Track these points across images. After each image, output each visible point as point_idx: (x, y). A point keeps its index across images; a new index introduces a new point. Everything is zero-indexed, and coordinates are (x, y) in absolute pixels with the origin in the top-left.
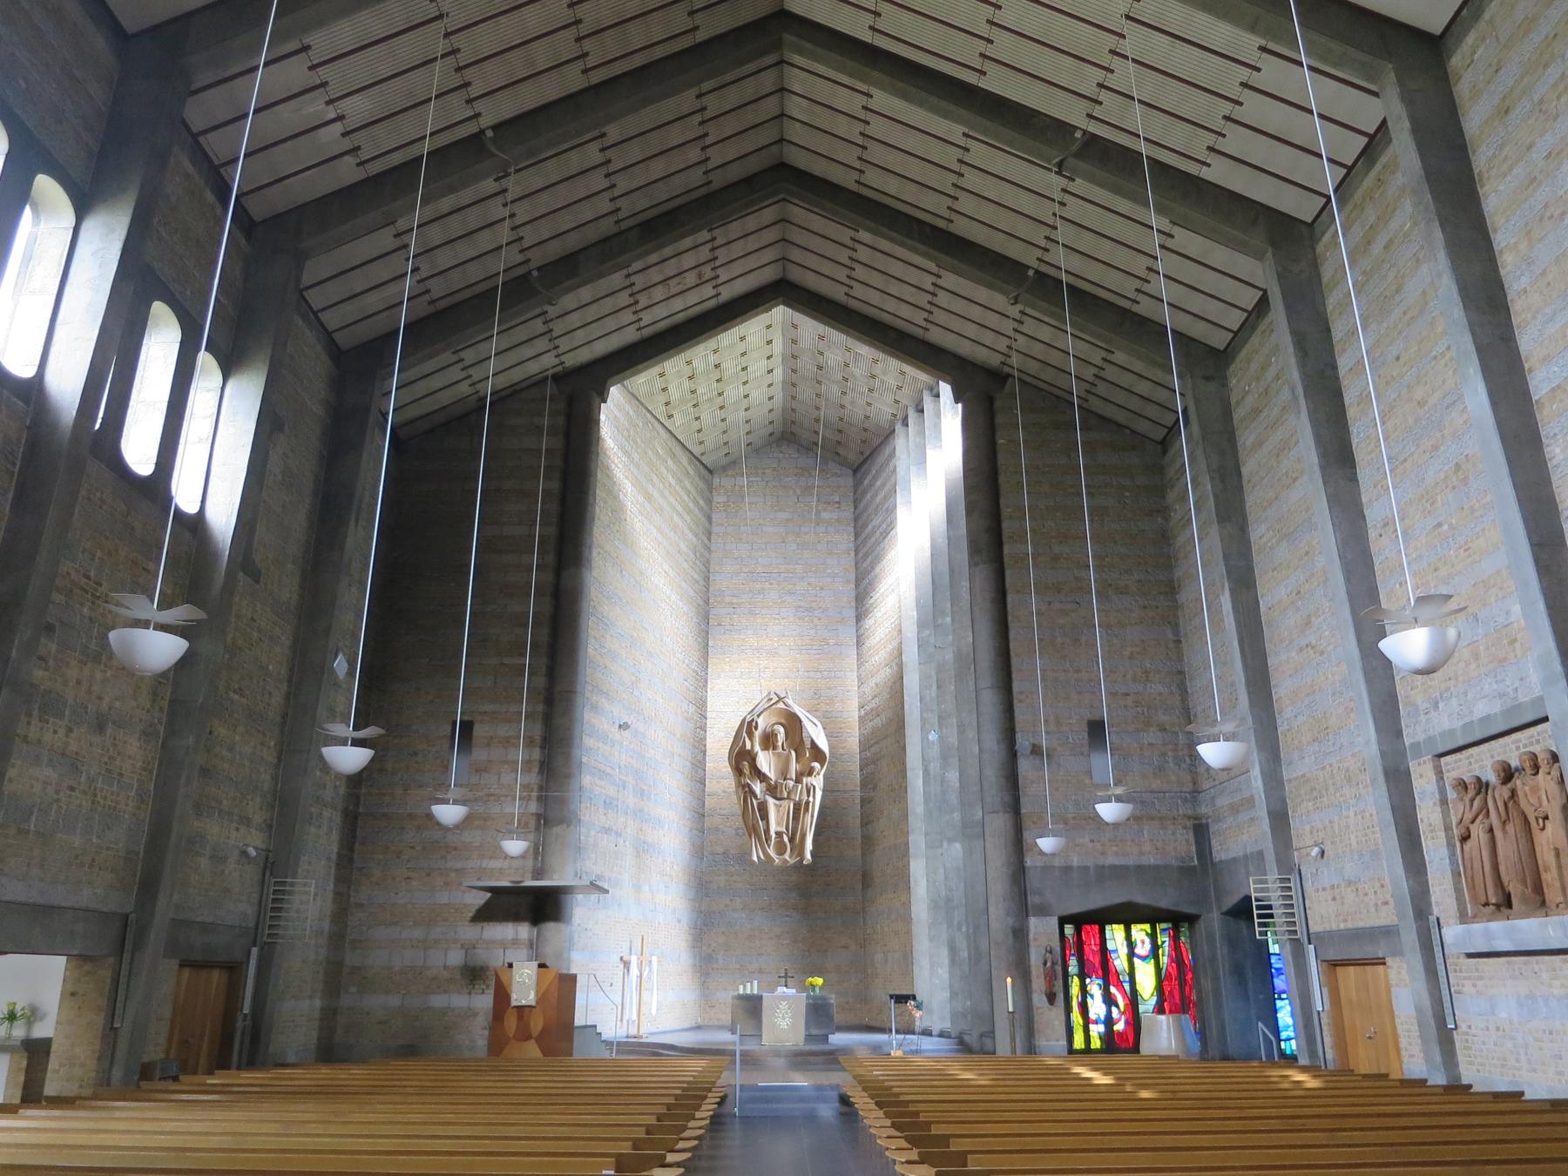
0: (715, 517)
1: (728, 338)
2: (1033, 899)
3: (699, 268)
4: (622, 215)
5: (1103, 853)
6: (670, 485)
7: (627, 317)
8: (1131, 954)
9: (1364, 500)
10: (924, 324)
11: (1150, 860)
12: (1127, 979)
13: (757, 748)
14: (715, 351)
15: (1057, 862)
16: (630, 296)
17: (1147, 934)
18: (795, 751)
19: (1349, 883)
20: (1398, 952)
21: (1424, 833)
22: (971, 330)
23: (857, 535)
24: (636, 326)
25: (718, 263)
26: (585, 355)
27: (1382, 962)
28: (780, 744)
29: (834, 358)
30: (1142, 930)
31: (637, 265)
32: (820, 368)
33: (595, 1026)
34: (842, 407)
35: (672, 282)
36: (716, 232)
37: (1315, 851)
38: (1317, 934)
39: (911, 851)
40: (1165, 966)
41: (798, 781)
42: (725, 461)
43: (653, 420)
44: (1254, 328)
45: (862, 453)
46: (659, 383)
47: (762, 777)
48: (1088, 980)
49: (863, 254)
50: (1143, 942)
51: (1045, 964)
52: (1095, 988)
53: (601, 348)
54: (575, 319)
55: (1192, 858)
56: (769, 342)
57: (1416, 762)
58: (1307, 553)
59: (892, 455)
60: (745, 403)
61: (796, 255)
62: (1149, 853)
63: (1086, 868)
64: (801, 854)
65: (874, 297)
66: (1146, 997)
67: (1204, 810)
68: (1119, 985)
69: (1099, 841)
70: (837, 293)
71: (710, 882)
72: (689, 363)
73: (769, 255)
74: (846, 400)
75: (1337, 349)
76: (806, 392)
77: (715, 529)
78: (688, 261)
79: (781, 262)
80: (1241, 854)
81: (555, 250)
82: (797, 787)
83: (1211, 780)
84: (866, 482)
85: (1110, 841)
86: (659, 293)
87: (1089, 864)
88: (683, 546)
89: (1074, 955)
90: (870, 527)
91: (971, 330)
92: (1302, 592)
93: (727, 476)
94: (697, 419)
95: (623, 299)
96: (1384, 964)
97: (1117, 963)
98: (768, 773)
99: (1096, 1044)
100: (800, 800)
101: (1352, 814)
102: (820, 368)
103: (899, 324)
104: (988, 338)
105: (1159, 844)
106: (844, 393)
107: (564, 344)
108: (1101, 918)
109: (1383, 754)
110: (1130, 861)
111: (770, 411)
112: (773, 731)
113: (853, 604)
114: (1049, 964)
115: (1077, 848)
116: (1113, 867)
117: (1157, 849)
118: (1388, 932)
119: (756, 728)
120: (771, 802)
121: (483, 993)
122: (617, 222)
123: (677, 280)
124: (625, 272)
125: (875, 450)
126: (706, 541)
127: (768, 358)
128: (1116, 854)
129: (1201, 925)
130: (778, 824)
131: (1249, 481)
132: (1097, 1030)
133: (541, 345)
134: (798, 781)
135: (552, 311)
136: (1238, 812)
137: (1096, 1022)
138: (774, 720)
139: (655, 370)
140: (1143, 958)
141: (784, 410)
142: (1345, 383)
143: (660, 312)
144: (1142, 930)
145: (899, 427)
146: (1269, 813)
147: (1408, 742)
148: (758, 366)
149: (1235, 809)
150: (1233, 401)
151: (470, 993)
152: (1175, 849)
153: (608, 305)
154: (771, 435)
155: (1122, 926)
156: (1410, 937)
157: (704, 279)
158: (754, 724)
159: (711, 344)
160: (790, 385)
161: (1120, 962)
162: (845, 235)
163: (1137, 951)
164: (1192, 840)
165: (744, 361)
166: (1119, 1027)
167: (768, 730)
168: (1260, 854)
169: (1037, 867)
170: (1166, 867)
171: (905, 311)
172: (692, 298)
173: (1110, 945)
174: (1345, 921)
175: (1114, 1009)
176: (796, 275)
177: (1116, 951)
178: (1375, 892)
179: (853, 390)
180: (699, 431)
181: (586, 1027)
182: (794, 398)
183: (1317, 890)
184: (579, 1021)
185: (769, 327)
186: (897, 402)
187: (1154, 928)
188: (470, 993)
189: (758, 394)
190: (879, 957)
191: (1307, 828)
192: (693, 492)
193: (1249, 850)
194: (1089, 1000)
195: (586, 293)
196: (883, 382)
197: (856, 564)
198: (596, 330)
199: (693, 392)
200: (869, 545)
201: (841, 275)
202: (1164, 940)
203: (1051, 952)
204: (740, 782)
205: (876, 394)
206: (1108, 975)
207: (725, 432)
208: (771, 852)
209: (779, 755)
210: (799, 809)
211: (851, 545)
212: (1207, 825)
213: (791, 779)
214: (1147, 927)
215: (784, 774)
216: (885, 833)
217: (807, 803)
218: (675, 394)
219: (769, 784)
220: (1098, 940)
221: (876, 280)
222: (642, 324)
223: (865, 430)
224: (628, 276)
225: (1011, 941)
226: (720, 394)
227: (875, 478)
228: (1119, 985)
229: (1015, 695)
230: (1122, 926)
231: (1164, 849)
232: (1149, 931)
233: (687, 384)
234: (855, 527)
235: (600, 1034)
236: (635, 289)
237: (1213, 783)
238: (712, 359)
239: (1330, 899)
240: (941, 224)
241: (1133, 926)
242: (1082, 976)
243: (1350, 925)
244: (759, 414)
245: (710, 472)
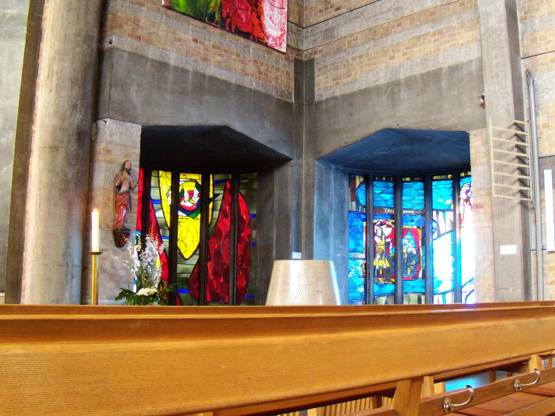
5: (205, 60)
8: (176, 207)
11: (251, 83)
12: (168, 234)
17: (197, 185)
30: (192, 180)
40: (215, 221)
50: (191, 193)
51: (119, 187)
63: (184, 71)
66: (187, 256)
69: (203, 44)
85: (214, 47)
97: (159, 214)
105: (263, 68)
110: (233, 78)
114: (124, 188)
115: (177, 44)
116: (212, 79)
117: (260, 73)
140: (189, 212)
144: (192, 180)
152: (277, 78)
155: (169, 175)
163: (182, 203)
169: (125, 51)
170: (267, 96)
173: (154, 194)
177: (160, 201)
187: (205, 180)
203: (129, 172)
214: (197, 177)
225: (73, 147)
230: (169, 175)
231: (267, 75)
241: (182, 176)
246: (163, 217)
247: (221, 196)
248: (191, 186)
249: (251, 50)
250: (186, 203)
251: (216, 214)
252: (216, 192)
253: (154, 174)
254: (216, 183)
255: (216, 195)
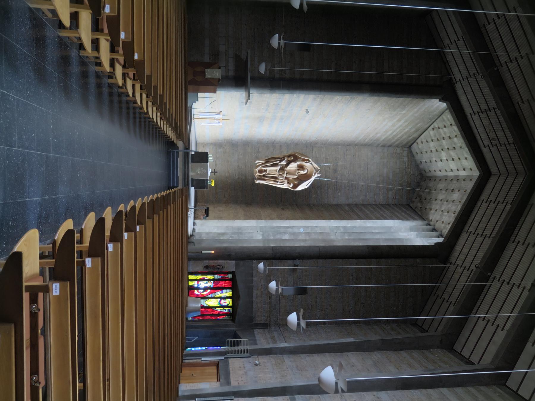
0: (391, 148)
1: (466, 152)
2: (241, 262)
3: (497, 138)
4: (521, 105)
6: (404, 129)
7: (476, 109)
8: (221, 298)
9: (389, 392)
10: (469, 231)
11: (255, 305)
12: (213, 296)
13: (298, 163)
14: (461, 147)
15: (254, 272)
16: (485, 110)
17: (228, 304)
18: (297, 178)
19: (246, 373)
20: (221, 385)
21: (263, 398)
22: (466, 250)
23: (382, 205)
24: (472, 113)
25: (499, 147)
26: (460, 92)
27: (218, 380)
28: (300, 172)
29: (456, 196)
30: (230, 302)
31: (498, 112)
32: (453, 190)
33: (198, 101)
34: (436, 200)
35: (491, 127)
36: (512, 145)
37: (257, 362)
38: (228, 361)
39: (259, 221)
40: (217, 310)
41: (286, 178)
42: (414, 152)
43: (432, 122)
44: (462, 360)
45: (416, 208)
46: (447, 124)
47: (287, 165)
48: (212, 282)
49: (501, 207)
50: (225, 303)
51: (218, 266)
52: (210, 284)
53: (463, 99)
54: (475, 87)
55: (255, 322)
56: (464, 170)
57: (288, 398)
58: (368, 370)
59: (414, 219)
60: (438, 160)
61: (502, 179)
62: (257, 306)
63: (252, 283)
64: (259, 179)
65: (481, 211)
66: (206, 302)
67: (273, 327)
68: (210, 293)
69: (262, 288)
70: (484, 196)
71: (248, 146)
72: (456, 136)
73: (502, 168)
74: (438, 201)
75: (451, 389)
76: (442, 185)
77: (386, 149)
78: (500, 134)
79: (498, 173)
80: (256, 338)
81: (507, 76)
82: (284, 178)
83: (284, 331)
84: (404, 209)
85: (262, 292)
86: (486, 122)
87: (254, 283)
88: (379, 135)
89: (221, 277)
90: (385, 210)
91: (466, 250)
92: (353, 367)
93: (408, 153)
94: (432, 141)
95: (484, 107)
96: (218, 381)
97: (218, 293)
98: (289, 167)
99: (190, 283)
100: (278, 179)
101: (270, 376)
102: (453, 190)
103: (469, 222)
104: (462, 257)
106: (441, 200)
107: (465, 83)
108: (234, 288)
109: (292, 387)
110: (254, 299)
111: (435, 171)
112: (305, 169)
113: (354, 203)
114: (218, 267)
115: (259, 280)
118: (228, 383)
119: (306, 163)
120: (278, 168)
121: (209, 59)
122: (518, 103)
123: (492, 129)
124: (496, 107)
125: (417, 212)
126: (381, 145)
127: (458, 170)
128: (257, 294)
129: (231, 323)
130: (270, 171)
131: (398, 353)
132: (195, 284)
133: (465, 73)
134: (286, 178)
135: (479, 77)
136: (272, 339)
137: (198, 284)
138: (309, 169)
139: (453, 122)
140: (220, 302)
141: (435, 176)
142: (437, 390)
143: (478, 123)
144: (230, 302)
145: (426, 222)
146: (271, 348)
147: (296, 396)
148: (454, 165)
149: (273, 338)
150: (432, 350)
151: (209, 54)
153: (481, 100)
154: (425, 171)
155: (231, 295)
156: (226, 389)
157: (492, 141)
158: (308, 162)
159: (464, 145)
160: (446, 178)
161: (219, 294)
162: (510, 199)
163: (222, 300)
164: (262, 322)
165: (456, 159)
166: (196, 292)
167: (305, 167)
168: (257, 344)
169: (253, 265)
171: (475, 224)
172: (484, 136)
173: (224, 291)
174: (233, 370)
175: (202, 291)
176: (493, 180)
178: (242, 381)
179: (443, 204)
180: (427, 141)
181: (198, 97)
182: (440, 180)
183: (243, 362)
184: (200, 94)
185: (471, 169)
186: (437, 221)
187: (230, 307)
188: (209, 54)
189: (442, 166)
190: (221, 208)
191: (265, 361)
192: (402, 139)
193: (257, 341)
194: (206, 282)
195: (487, 91)
196: (446, 216)
197: (370, 205)
198: (471, 96)
199: (444, 138)
200: (377, 209)
201: (492, 198)
202: (226, 310)
204: (286, 156)
205: (440, 213)
206: (215, 289)
207: (426, 152)
208: (259, 168)
209: (295, 171)
210: (275, 179)
211: (378, 203)
212: (268, 328)
213: (286, 176)
214: (231, 305)
215: (289, 173)
216: (266, 212)
217: (277, 182)
218: (443, 130)
219: (284, 168)
220: (226, 286)
221: (489, 212)
222: (473, 116)
223: (426, 209)
224: (494, 108)
226: (442, 150)
227: (405, 212)
228: (210, 293)
229: (317, 260)
230: (231, 295)
232: (229, 305)
233: (447, 136)
234: (385, 204)
235: (195, 103)
236: (488, 112)
237: (282, 331)
238: (457, 146)
239: (240, 366)
240: (512, 239)
241: (231, 299)
242: (214, 280)
243: (231, 372)
244: (433, 167)
245: (410, 146)
246: (219, 300)
247: (225, 311)
248: (228, 303)
249: (265, 305)
250: (222, 301)
251: (220, 310)
252: (226, 310)
253: (231, 290)
254: (229, 310)
255: (225, 310)
